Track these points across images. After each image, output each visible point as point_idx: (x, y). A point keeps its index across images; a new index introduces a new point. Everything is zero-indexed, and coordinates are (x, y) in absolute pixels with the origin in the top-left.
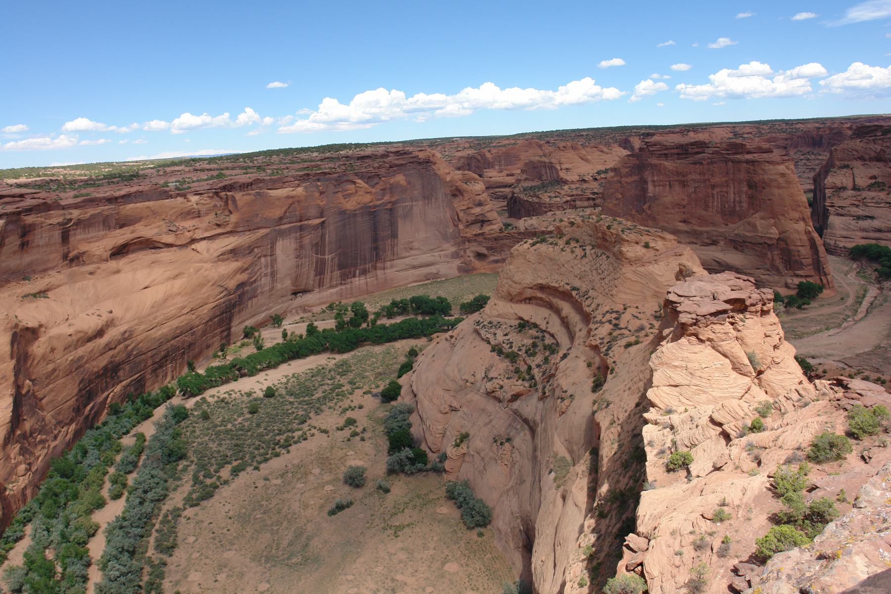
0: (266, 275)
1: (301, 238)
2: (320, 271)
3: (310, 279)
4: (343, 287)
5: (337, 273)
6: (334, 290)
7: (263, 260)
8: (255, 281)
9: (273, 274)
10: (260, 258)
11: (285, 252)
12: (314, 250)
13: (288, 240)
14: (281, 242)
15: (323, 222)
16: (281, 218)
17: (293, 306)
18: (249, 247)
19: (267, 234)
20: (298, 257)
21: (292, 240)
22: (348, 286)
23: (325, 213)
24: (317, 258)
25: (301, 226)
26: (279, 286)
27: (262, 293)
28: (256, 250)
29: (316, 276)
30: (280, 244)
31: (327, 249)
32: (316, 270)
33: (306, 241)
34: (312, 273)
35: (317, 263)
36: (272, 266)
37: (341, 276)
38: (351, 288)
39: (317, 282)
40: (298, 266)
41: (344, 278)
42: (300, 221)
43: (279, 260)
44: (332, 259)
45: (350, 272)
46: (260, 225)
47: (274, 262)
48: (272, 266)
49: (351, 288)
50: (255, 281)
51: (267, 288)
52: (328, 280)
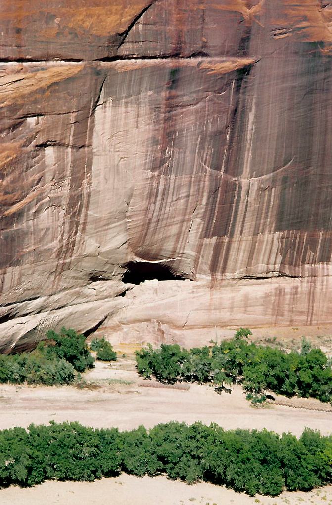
0: (55, 203)
1: (171, 107)
2: (220, 223)
3: (187, 242)
4: (287, 284)
5: (271, 239)
6: (257, 290)
7: (49, 151)
8: (19, 215)
9: (77, 204)
10: (44, 145)
11: (121, 131)
12: (208, 152)
13: (132, 110)
14: (109, 111)
15: (244, 71)
16: (121, 38)
17: (128, 314)
18: (13, 109)
19: (70, 80)
20: (158, 165)
21: (145, 110)
22: (303, 285)
23: (254, 43)
24: (215, 179)
25: (175, 72)
26: (90, 244)
27: (39, 254)
28: (31, 121)
29: (206, 234)
30: (103, 116)
31: (248, 157)
32: (209, 216)
33: (188, 121)
34: (197, 224)
35: (213, 192)
36: (77, 181)
37: (283, 251)
38: (311, 295)
39: (208, 254)
40: (152, 195)
41: (292, 259)
42: (176, 55)
43: (98, 164)
44: (262, 190)
45: (312, 242)
46: (52, 52)
47: (81, 170)
48: (77, 181)
49: (311, 295)
50: (19, 215)
51: (55, 244)
52: (243, 256)
